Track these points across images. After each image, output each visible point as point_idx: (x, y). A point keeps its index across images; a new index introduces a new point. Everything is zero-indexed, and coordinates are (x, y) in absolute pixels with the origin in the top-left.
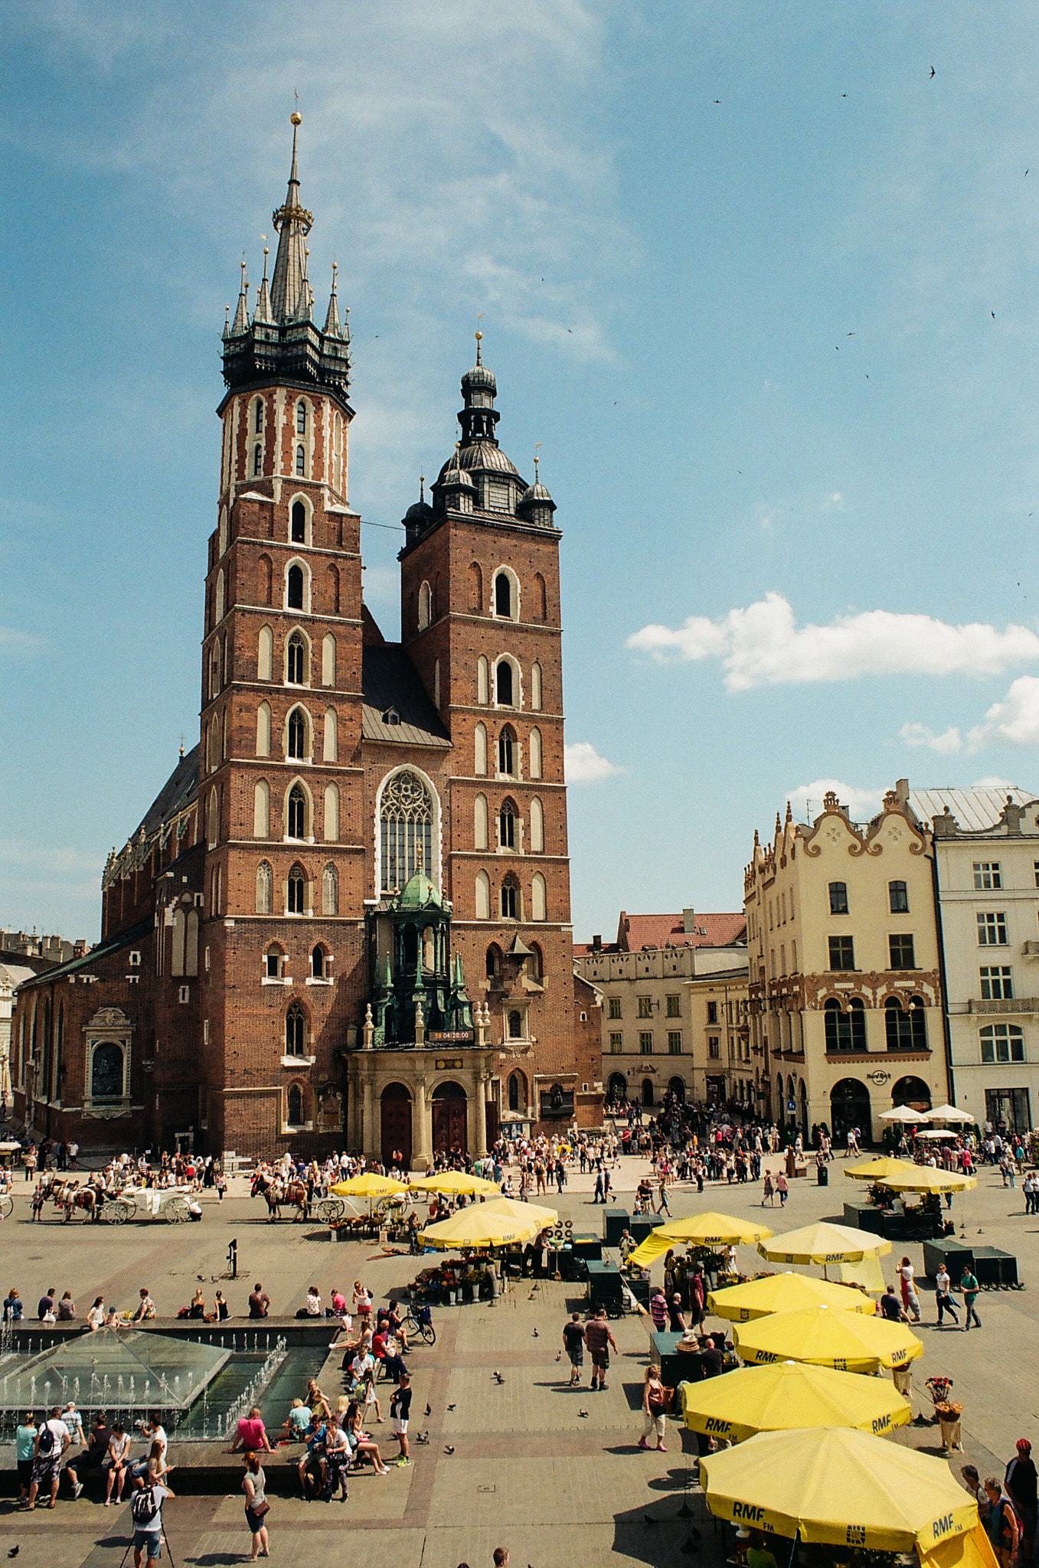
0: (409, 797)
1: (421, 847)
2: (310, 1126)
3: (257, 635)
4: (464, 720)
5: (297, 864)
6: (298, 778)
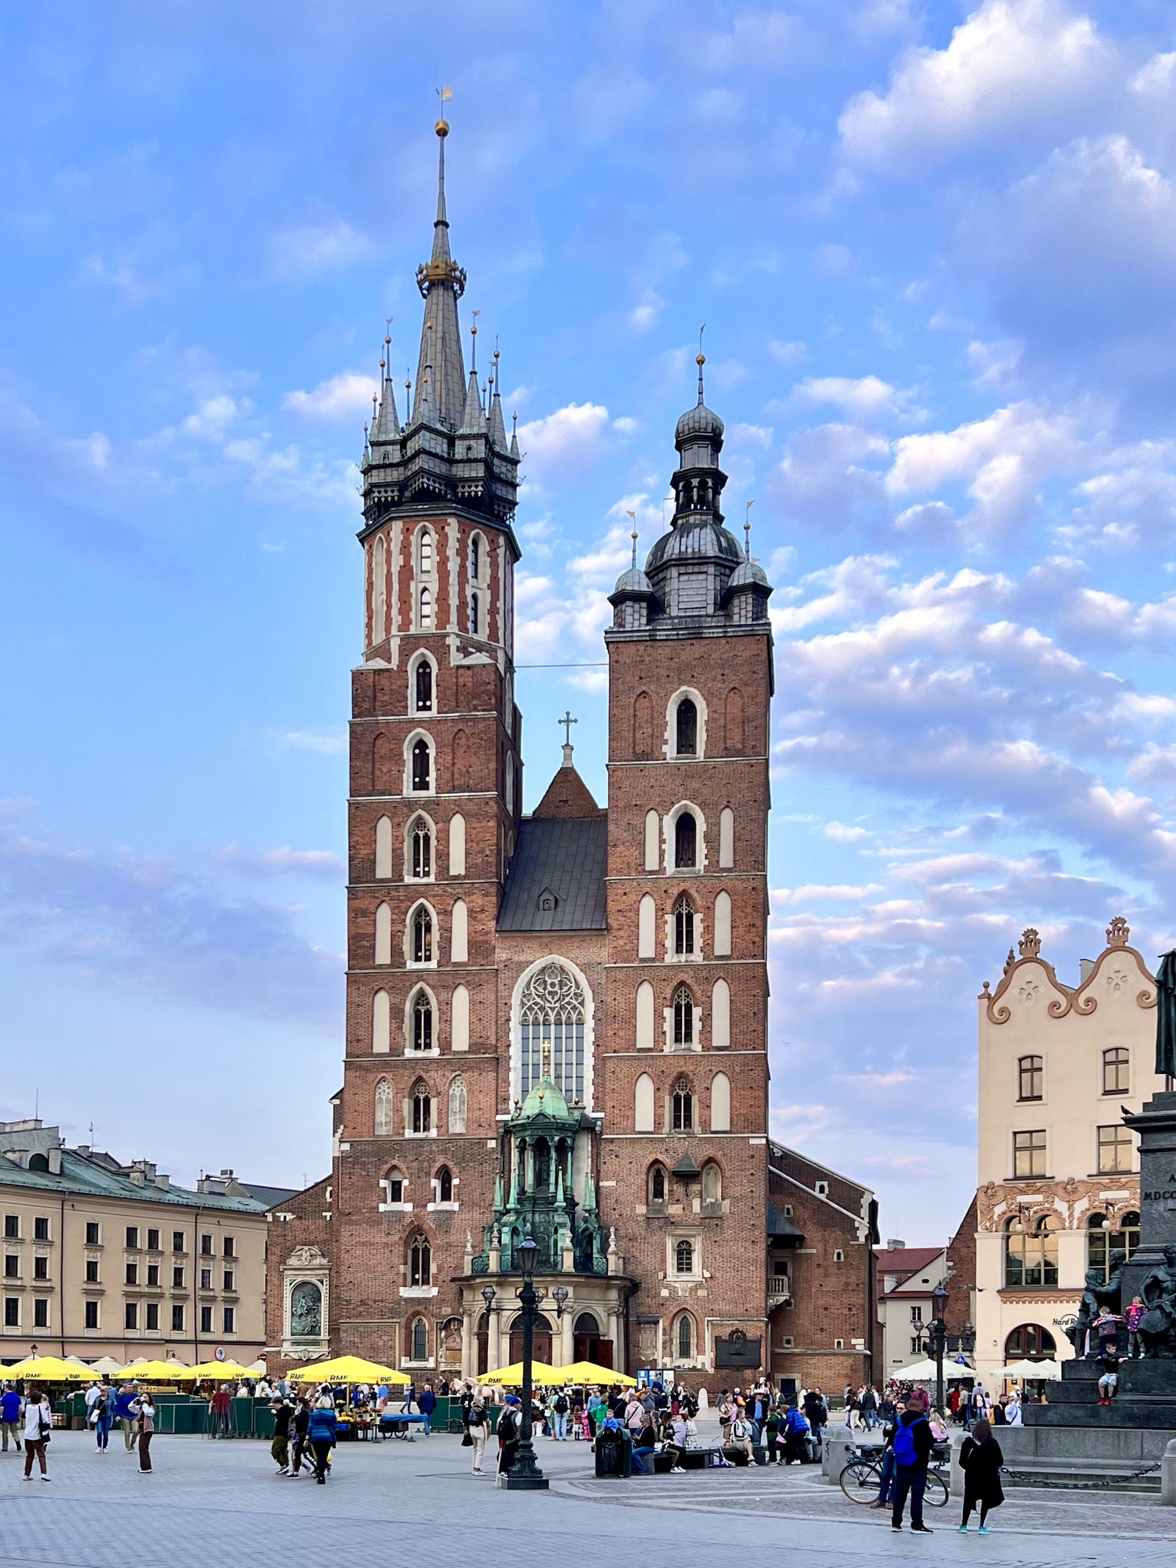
0: (556, 993)
1: (549, 1051)
2: (431, 1363)
3: (374, 829)
4: (625, 894)
5: (420, 1079)
6: (421, 984)
